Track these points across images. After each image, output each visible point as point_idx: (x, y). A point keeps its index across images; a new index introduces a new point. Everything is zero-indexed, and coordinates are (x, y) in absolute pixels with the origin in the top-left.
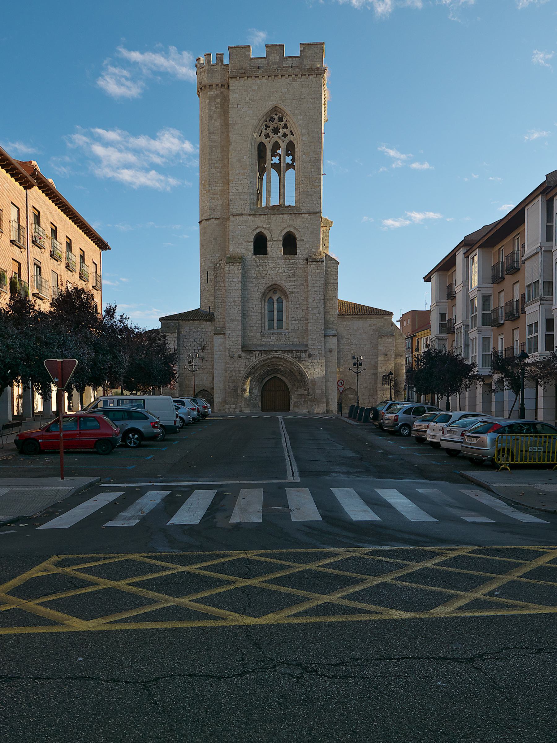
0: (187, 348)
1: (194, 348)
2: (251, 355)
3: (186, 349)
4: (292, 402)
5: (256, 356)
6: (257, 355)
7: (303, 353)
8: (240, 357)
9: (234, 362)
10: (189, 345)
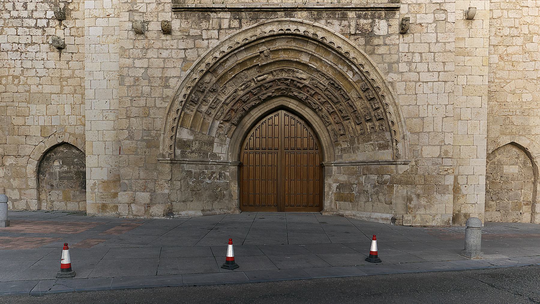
0: (14, 14)
1: (36, 15)
2: (204, 25)
3: (12, 17)
4: (330, 186)
5: (220, 29)
6: (225, 24)
7: (379, 18)
8: (167, 31)
9: (146, 49)
10: (19, 6)
